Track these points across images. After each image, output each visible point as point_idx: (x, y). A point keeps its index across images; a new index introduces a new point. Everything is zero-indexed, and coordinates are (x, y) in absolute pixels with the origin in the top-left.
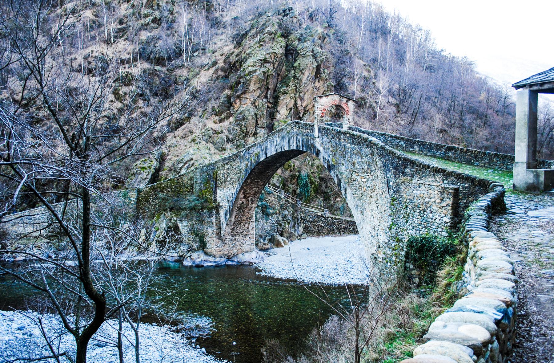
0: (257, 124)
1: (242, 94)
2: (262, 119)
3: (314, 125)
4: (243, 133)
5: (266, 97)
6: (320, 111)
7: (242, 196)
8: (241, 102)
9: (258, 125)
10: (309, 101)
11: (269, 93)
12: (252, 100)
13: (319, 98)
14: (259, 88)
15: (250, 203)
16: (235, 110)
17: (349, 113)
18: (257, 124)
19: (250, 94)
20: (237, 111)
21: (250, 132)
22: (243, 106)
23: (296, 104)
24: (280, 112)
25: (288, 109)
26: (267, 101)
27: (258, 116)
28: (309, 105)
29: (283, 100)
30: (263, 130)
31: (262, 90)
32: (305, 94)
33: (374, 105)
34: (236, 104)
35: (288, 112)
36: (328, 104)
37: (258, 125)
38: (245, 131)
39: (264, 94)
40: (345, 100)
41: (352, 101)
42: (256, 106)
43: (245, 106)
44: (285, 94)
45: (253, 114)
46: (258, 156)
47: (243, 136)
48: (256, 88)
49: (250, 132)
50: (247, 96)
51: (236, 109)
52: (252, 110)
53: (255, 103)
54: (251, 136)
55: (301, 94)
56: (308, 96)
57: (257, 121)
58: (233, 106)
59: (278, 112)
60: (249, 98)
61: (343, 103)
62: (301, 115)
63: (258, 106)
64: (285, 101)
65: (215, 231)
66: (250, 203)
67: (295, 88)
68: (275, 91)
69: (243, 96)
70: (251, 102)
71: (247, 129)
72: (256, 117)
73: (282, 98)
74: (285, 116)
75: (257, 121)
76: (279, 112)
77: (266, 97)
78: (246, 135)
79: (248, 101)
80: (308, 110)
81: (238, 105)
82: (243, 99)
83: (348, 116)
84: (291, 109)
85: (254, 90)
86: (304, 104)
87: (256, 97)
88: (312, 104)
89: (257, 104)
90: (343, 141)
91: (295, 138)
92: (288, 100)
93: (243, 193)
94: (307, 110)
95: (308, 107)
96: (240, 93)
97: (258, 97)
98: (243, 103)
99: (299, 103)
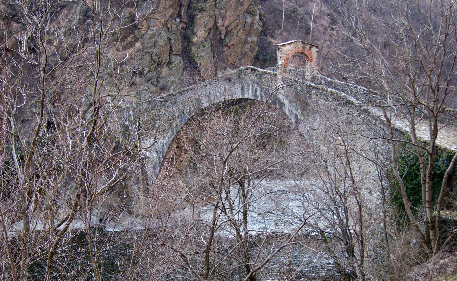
2: (177, 44)
3: (276, 75)
5: (179, 16)
6: (283, 61)
7: (175, 146)
8: (148, 24)
10: (232, 19)
11: (183, 11)
12: (163, 20)
13: (282, 47)
14: (171, 6)
15: (183, 153)
17: (313, 61)
19: (160, 14)
20: (144, 35)
22: (152, 28)
23: (216, 23)
24: (198, 34)
25: (207, 29)
26: (181, 20)
27: (173, 41)
28: (232, 24)
31: (174, 7)
32: (226, 11)
33: (306, 17)
35: (207, 34)
36: (291, 52)
37: (173, 51)
39: (177, 12)
40: (308, 47)
41: (315, 47)
42: (168, 28)
43: (155, 29)
44: (202, 11)
46: (198, 101)
48: (168, 6)
50: (158, 16)
51: (143, 32)
52: (163, 33)
53: (167, 25)
54: (164, 66)
55: (222, 11)
56: (231, 12)
57: (171, 47)
58: (139, 29)
59: (194, 33)
60: (159, 18)
61: (306, 50)
62: (223, 37)
63: (171, 27)
64: (203, 21)
65: (141, 187)
66: (183, 153)
67: (214, 3)
68: (189, 7)
70: (162, 24)
71: (159, 58)
73: (199, 17)
74: (203, 39)
75: (171, 47)
76: (196, 34)
78: (158, 64)
79: (158, 23)
80: (231, 31)
81: (145, 27)
82: (152, 20)
83: (312, 63)
84: (210, 29)
85: (166, 9)
86: (226, 23)
87: (168, 16)
88: (235, 23)
90: (314, 96)
91: (251, 87)
92: (206, 19)
93: (177, 143)
94: (229, 29)
95: (230, 27)
97: (170, 17)
98: (151, 25)
99: (220, 22)
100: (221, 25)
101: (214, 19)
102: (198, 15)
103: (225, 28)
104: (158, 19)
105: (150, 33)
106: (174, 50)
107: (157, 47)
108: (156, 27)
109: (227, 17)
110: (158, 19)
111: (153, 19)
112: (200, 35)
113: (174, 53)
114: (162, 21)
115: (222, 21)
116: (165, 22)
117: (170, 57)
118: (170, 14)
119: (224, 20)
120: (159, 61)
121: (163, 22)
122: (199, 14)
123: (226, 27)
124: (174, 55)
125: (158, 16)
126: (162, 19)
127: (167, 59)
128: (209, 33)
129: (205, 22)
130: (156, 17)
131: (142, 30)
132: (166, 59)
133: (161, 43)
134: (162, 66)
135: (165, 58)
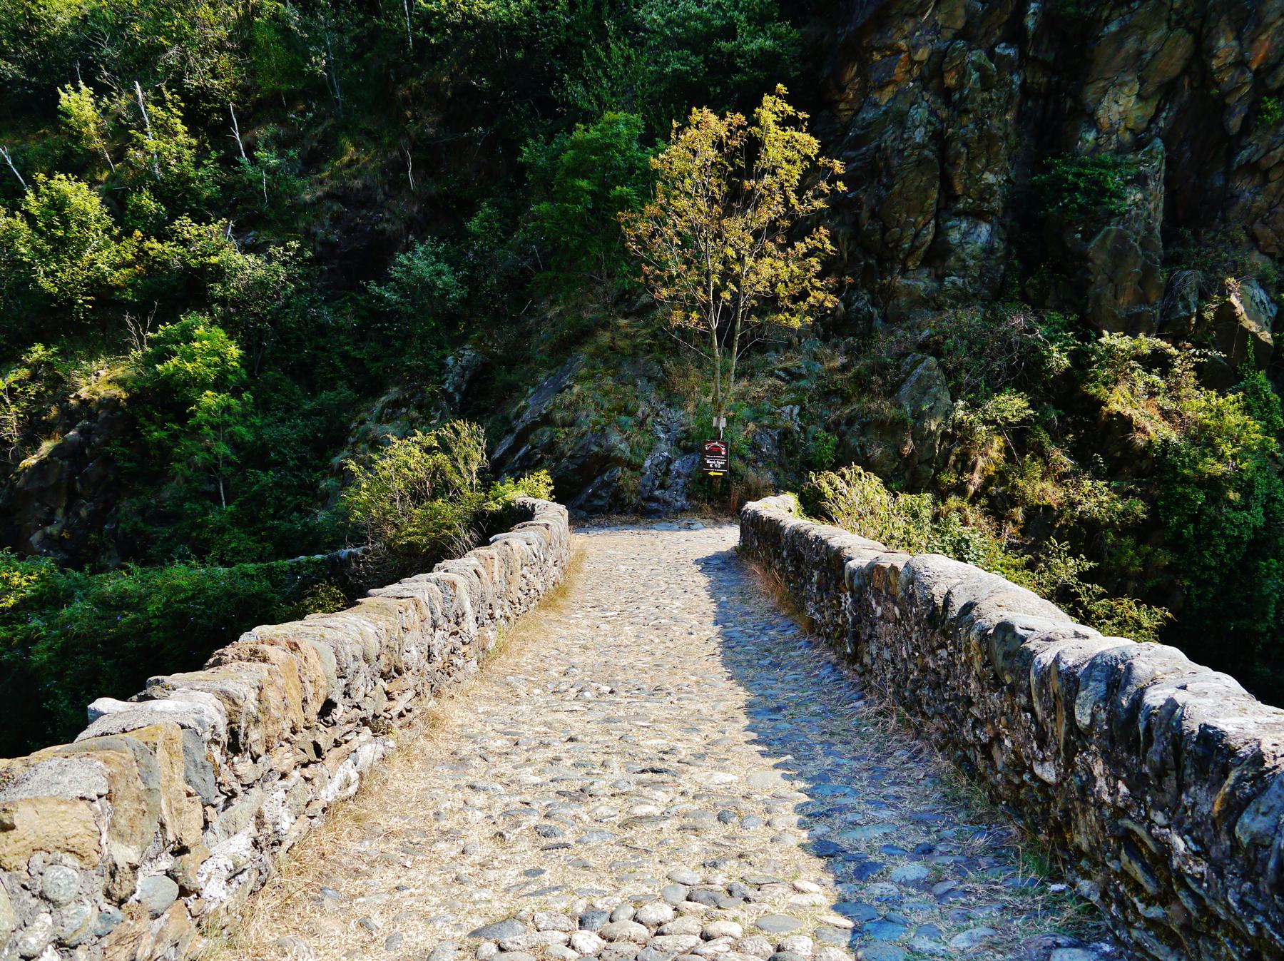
0: (949, 196)
9: (956, 199)
12: (922, 54)
18: (949, 196)
19: (908, 27)
20: (846, 128)
23: (1201, 52)
26: (1023, 54)
29: (1120, 38)
34: (842, 89)
35: (1150, 110)
54: (910, 265)
64: (1131, 45)
71: (885, 229)
73: (1113, 27)
74: (1127, 137)
77: (1015, 34)
78: (881, 261)
89: (951, 80)
99: (1225, 46)
100: (1230, 59)
101: (1189, 38)
102: (1107, 22)
103: (1249, 76)
105: (869, 115)
106: (959, 189)
108: (890, 88)
109: (1270, 18)
112: (1115, 118)
114: (916, 58)
115: (1238, 38)
116: (935, 59)
117: (937, 226)
118: (960, 24)
119: (1246, 33)
121: (920, 63)
122: (1116, 13)
123: (1257, 73)
124: (959, 214)
125: (899, 35)
126: (915, 48)
128: (1159, 110)
129: (1140, 53)
130: (889, 42)
131: (842, 106)
132: (917, 235)
134: (898, 267)
135: (913, 231)
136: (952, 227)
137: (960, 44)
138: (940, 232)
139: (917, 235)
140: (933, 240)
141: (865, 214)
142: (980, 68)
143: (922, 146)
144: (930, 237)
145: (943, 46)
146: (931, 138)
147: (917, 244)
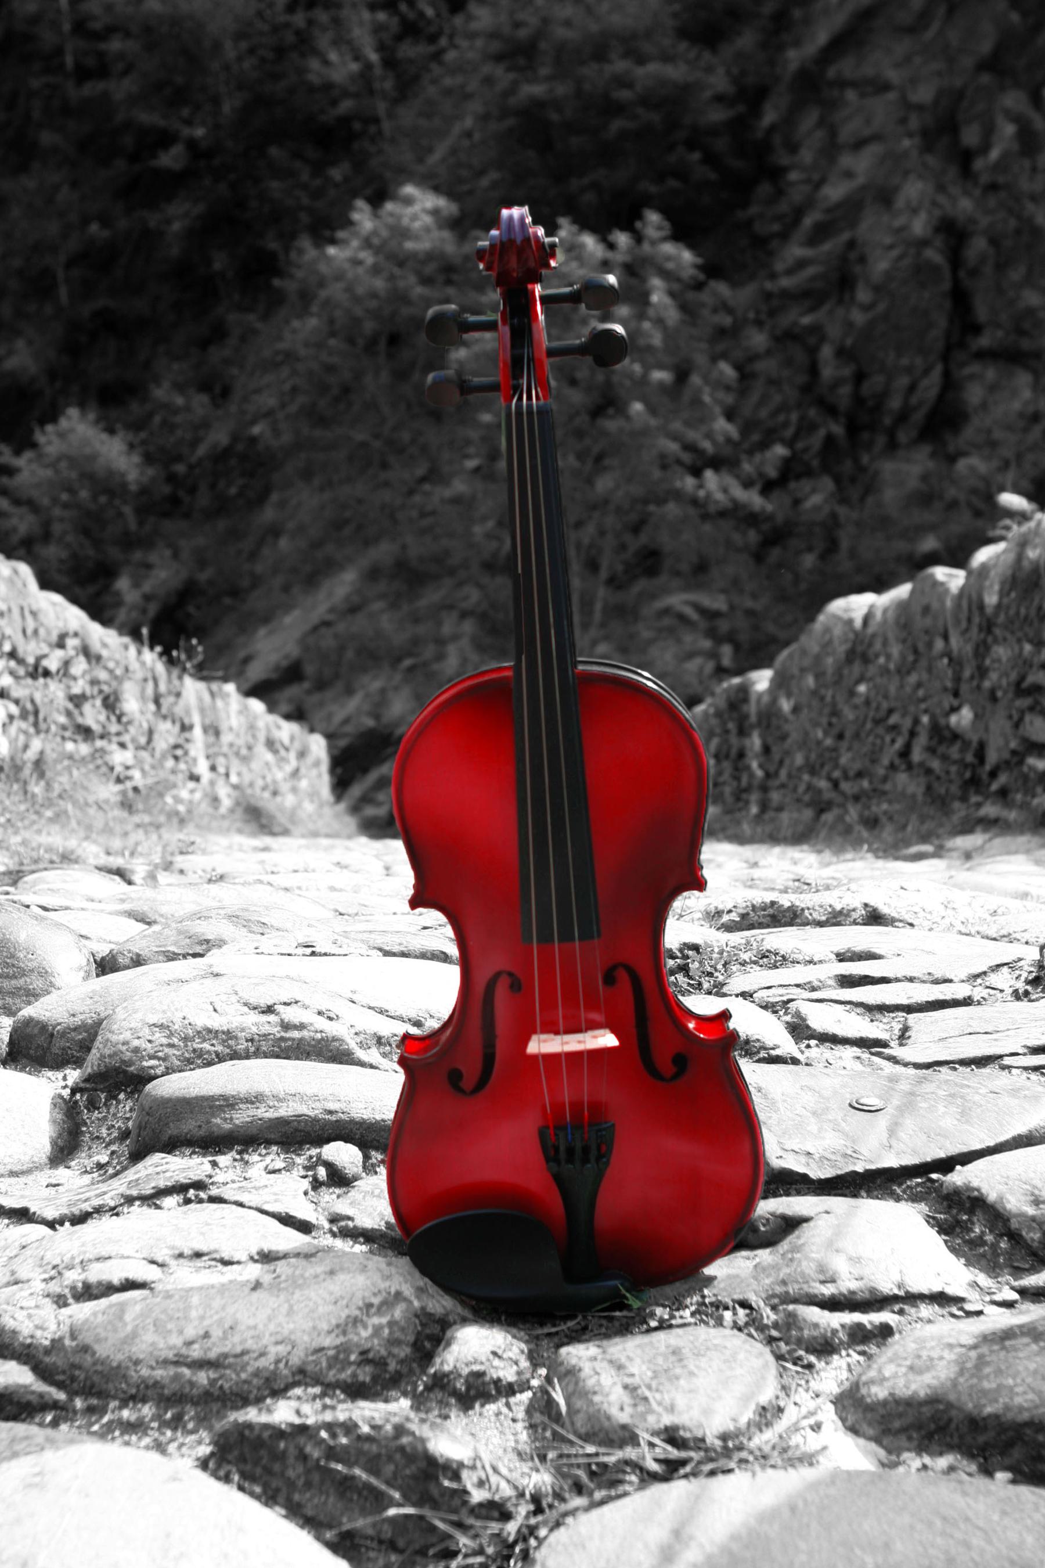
1: (838, 45)
2: (1016, 274)
4: (832, 411)
8: (833, 133)
9: (976, 329)
12: (924, 94)
16: (783, 207)
20: (799, 213)
21: (895, 403)
27: (978, 246)
30: (1023, 379)
34: (793, 148)
38: (845, 391)
45: (919, 226)
47: (830, 440)
49: (895, 403)
54: (902, 437)
60: (893, 75)
69: (845, 67)
70: (914, 122)
71: (860, 377)
72: (955, 258)
78: (853, 429)
81: (806, 155)
82: (851, 95)
87: (968, 62)
96: (822, 37)
98: (846, 133)
104: (885, 87)
105: (834, 192)
106: (982, 312)
107: (863, 295)
110: (885, 87)
111: (853, 84)
113: (984, 341)
117: (947, 374)
118: (986, 47)
120: (858, 400)
121: (920, 108)
124: (981, 355)
127: (925, 383)
131: (793, 176)
132: (912, 388)
133: (881, 265)
134: (881, 440)
135: (904, 381)
136: (972, 377)
137: (985, 79)
138: (950, 384)
139: (912, 388)
140: (941, 397)
141: (827, 352)
142: (1018, 119)
143: (924, 243)
144: (933, 393)
145: (958, 82)
146: (937, 230)
147: (914, 400)
